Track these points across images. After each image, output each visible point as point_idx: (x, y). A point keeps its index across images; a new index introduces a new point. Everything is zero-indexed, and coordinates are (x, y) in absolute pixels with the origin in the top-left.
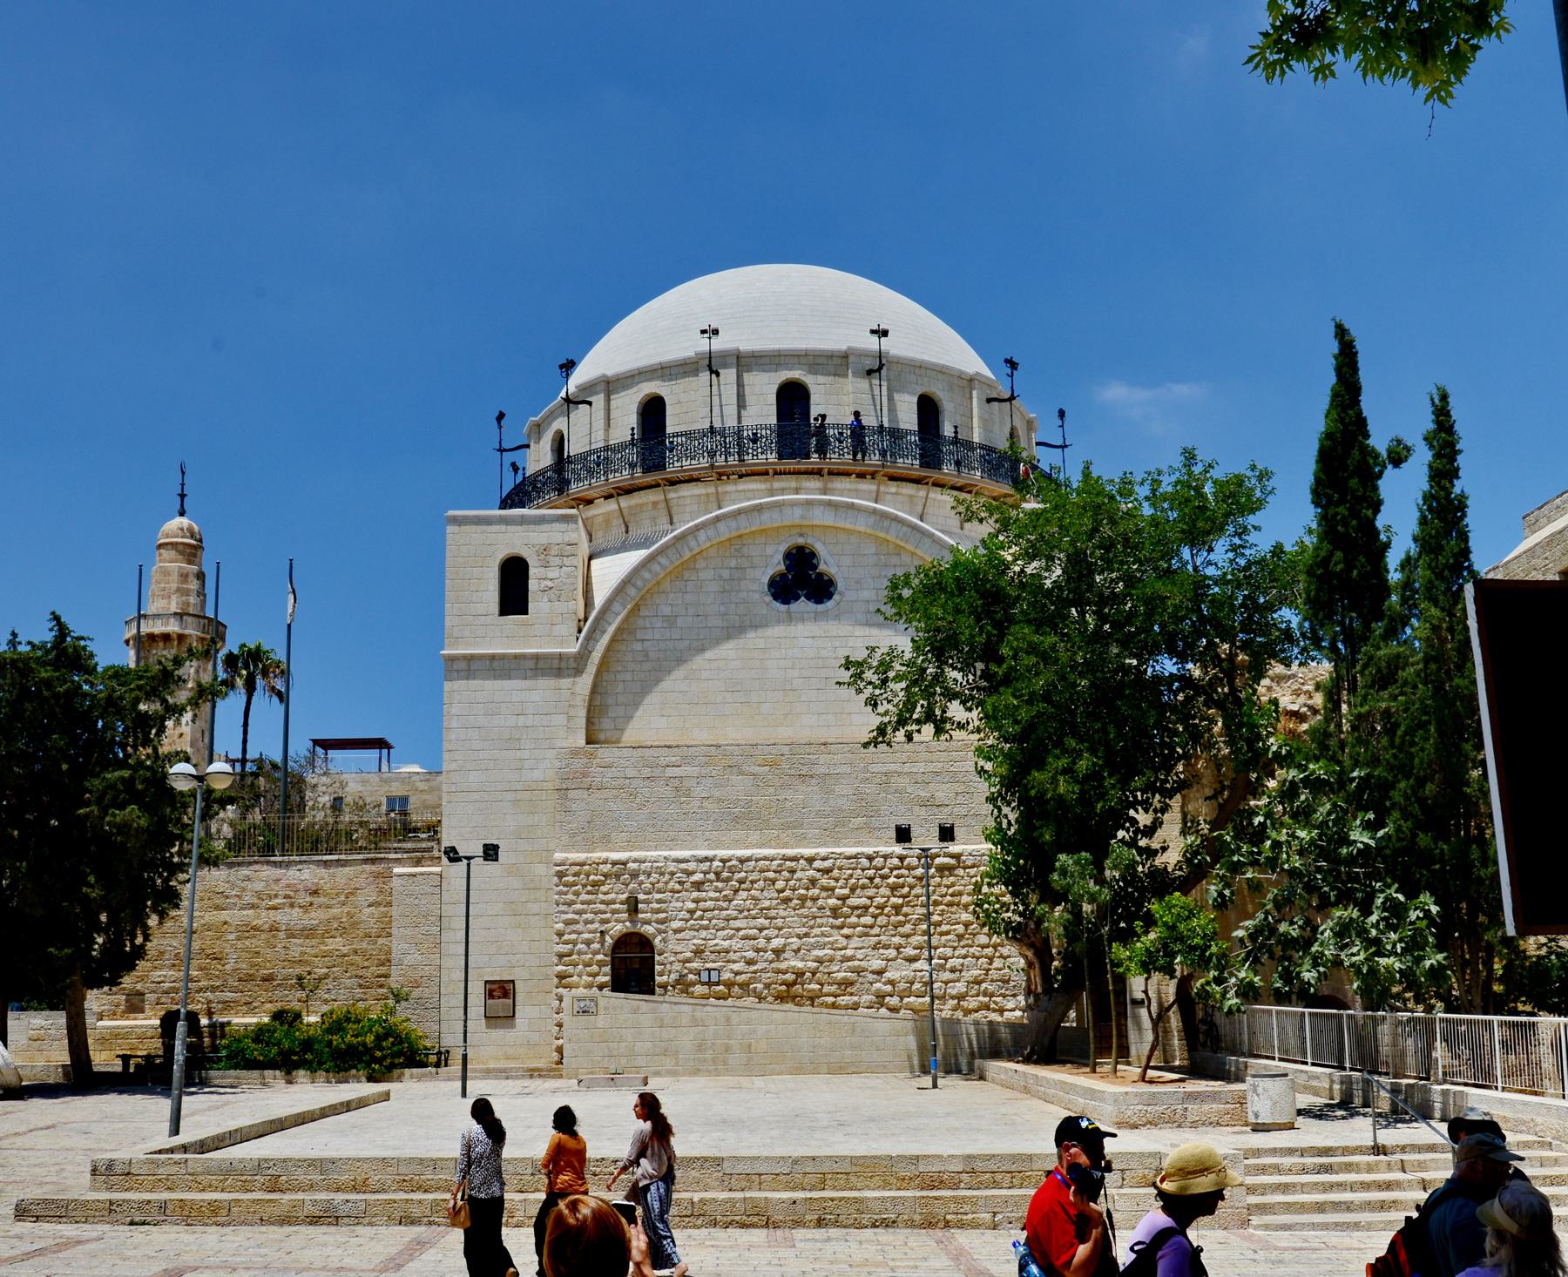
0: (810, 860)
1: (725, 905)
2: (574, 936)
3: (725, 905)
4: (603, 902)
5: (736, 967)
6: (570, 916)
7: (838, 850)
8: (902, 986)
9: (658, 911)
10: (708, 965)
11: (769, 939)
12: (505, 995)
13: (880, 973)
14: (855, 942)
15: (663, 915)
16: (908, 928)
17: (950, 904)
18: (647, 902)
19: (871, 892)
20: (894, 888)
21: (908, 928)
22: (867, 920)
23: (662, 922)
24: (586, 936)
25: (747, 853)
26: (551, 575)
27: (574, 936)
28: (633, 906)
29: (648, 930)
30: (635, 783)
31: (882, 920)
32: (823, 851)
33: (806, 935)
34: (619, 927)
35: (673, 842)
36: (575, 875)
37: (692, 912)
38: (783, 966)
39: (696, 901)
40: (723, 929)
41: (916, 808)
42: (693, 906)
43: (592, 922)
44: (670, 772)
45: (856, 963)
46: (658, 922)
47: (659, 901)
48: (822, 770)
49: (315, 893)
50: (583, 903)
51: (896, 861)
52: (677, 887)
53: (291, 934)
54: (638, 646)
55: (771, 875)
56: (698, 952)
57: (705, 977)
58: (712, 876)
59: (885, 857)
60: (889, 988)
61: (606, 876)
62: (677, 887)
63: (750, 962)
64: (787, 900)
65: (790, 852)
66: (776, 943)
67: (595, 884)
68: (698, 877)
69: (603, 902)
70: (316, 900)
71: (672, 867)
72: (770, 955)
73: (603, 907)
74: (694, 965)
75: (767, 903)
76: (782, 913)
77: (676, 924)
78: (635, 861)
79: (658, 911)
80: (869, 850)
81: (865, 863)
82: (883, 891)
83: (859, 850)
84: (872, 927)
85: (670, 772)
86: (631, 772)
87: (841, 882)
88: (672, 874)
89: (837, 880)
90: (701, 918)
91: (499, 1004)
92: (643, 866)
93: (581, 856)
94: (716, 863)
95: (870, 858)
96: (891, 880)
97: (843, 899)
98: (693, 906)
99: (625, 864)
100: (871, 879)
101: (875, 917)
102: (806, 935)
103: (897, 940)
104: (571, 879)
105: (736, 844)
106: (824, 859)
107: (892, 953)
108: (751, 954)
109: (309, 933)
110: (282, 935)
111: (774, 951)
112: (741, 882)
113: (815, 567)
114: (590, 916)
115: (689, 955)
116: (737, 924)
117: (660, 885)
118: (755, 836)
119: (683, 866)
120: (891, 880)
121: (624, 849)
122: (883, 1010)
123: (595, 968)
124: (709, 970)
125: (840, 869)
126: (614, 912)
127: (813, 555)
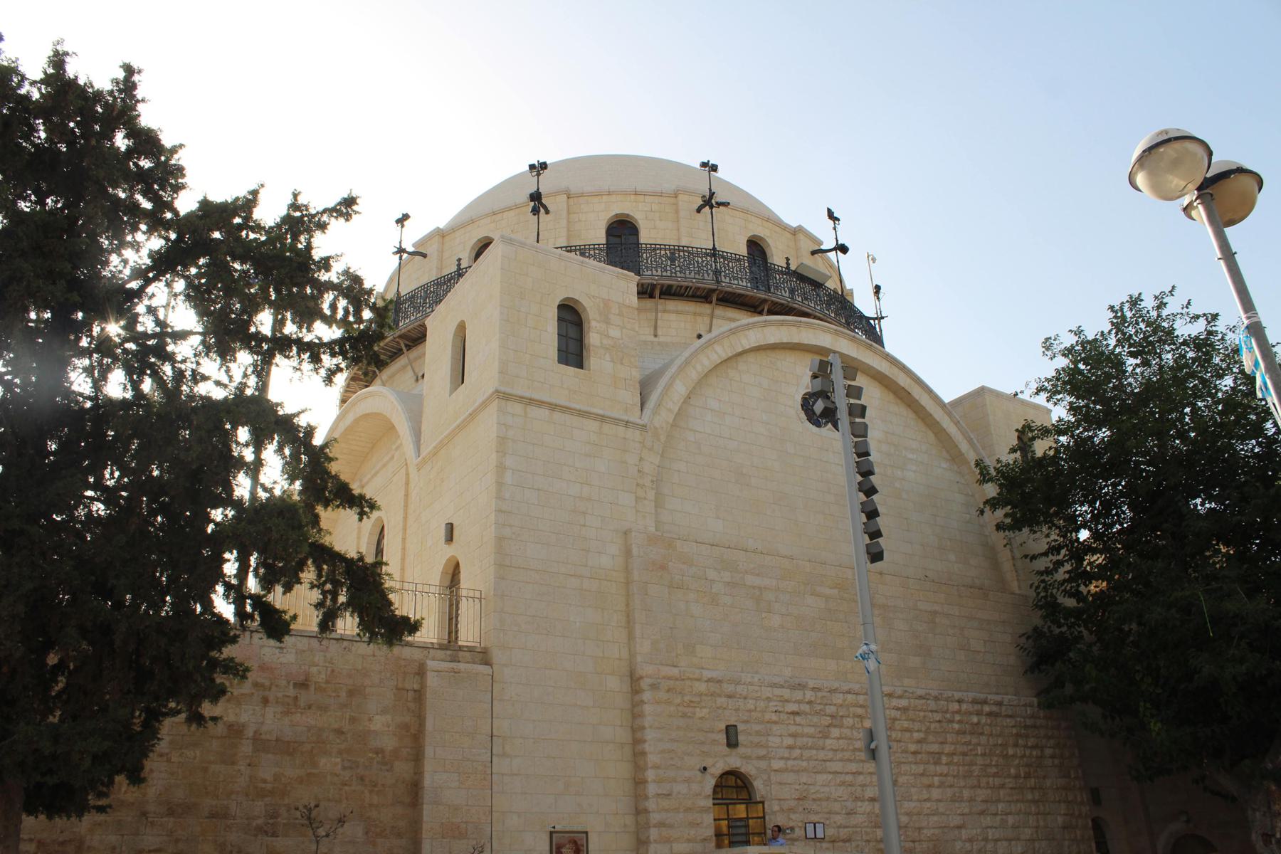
1: (821, 742)
5: (839, 819)
9: (758, 745)
13: (959, 827)
14: (936, 793)
15: (762, 752)
20: (959, 732)
22: (944, 769)
24: (687, 774)
25: (836, 685)
29: (747, 769)
32: (899, 691)
37: (790, 748)
39: (794, 736)
44: (751, 580)
46: (759, 758)
47: (758, 733)
49: (303, 685)
51: (956, 706)
52: (774, 717)
53: (260, 744)
55: (860, 711)
61: (701, 695)
63: (850, 813)
68: (794, 707)
69: (700, 730)
70: (304, 698)
71: (767, 692)
77: (777, 764)
86: (712, 574)
90: (801, 758)
98: (790, 741)
106: (900, 697)
108: (850, 805)
109: (285, 748)
110: (246, 748)
112: (832, 716)
115: (793, 803)
116: (837, 766)
119: (778, 692)
120: (956, 726)
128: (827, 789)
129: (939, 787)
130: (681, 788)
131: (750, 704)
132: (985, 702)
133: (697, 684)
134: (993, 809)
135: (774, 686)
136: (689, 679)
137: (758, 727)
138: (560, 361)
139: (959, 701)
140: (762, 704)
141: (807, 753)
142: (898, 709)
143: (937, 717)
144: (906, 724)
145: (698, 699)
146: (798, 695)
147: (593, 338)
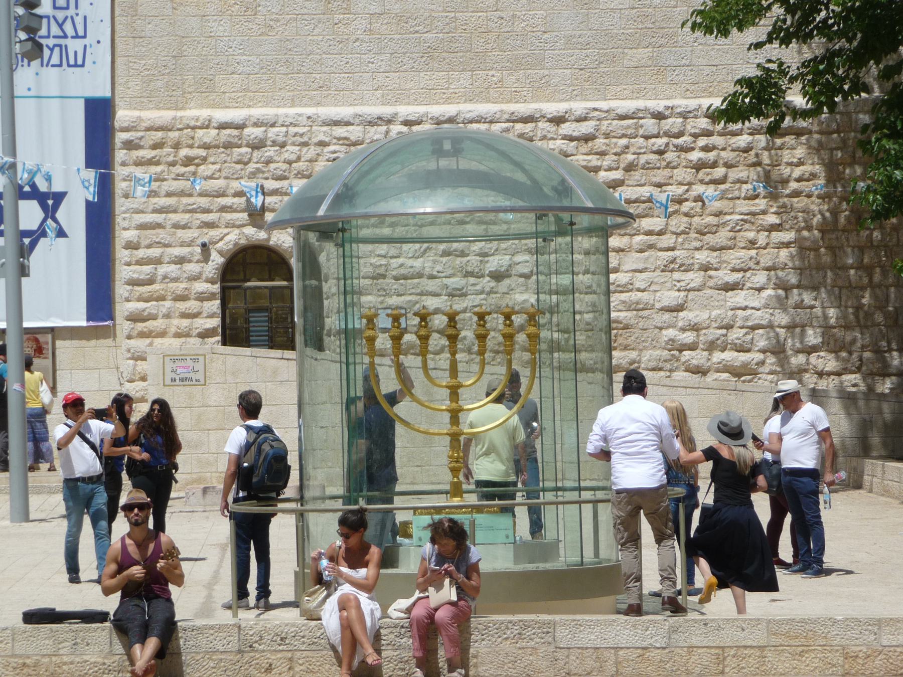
0: (558, 120)
2: (155, 252)
7: (604, 105)
8: (714, 333)
16: (722, 237)
19: (660, 176)
20: (699, 166)
21: (722, 237)
24: (177, 251)
25: (450, 110)
31: (678, 223)
32: (579, 107)
36: (155, 147)
45: (635, 296)
50: (169, 195)
59: (685, 115)
60: (688, 337)
61: (206, 146)
65: (523, 109)
67: (189, 161)
72: (487, 283)
73: (204, 202)
80: (658, 105)
81: (650, 124)
82: (681, 174)
83: (640, 104)
84: (661, 233)
87: (607, 161)
88: (322, 144)
92: (272, 133)
93: (165, 116)
95: (659, 116)
99: (241, 127)
103: (702, 257)
104: (147, 154)
105: (429, 95)
106: (580, 120)
107: (694, 278)
108: (456, 282)
114: (183, 218)
117: (301, 165)
118: (463, 81)
119: (340, 131)
120: (695, 156)
121: (238, 104)
122: (680, 376)
123: (192, 305)
125: (607, 136)
126: (224, 209)
129: (641, 251)
130: (172, 270)
131: (291, 151)
133: (200, 133)
135: (337, 123)
140: (311, 152)
142: (571, 139)
143: (661, 142)
144: (580, 159)
145: (202, 153)
146: (376, 133)
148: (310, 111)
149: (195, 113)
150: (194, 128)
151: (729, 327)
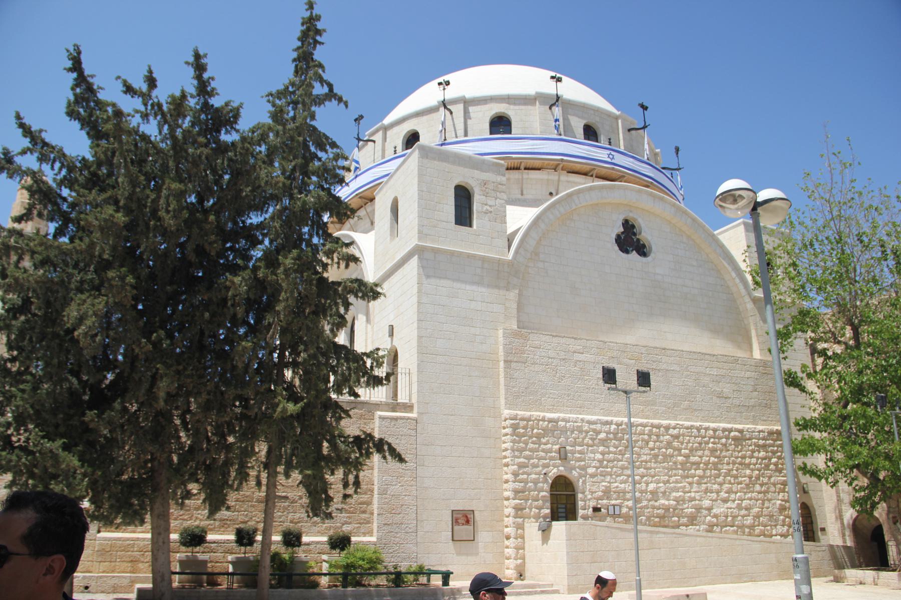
3: (620, 457)
4: (543, 451)
6: (522, 460)
9: (580, 460)
10: (613, 502)
11: (647, 484)
12: (468, 522)
13: (709, 509)
17: (741, 464)
18: (573, 452)
21: (721, 479)
23: (584, 468)
24: (533, 476)
26: (490, 203)
27: (525, 476)
28: (563, 455)
30: (555, 362)
31: (708, 473)
32: (673, 423)
33: (668, 482)
34: (555, 470)
35: (581, 409)
38: (657, 504)
39: (603, 454)
40: (620, 475)
41: (714, 398)
42: (600, 457)
43: (537, 466)
47: (580, 452)
48: (664, 366)
51: (711, 432)
54: (541, 265)
56: (607, 493)
57: (611, 512)
58: (611, 436)
62: (590, 442)
64: (656, 456)
65: (656, 422)
66: (652, 486)
67: (539, 436)
69: (543, 451)
72: (649, 496)
73: (543, 454)
74: (605, 501)
75: (644, 458)
76: (653, 465)
77: (591, 470)
78: (564, 420)
79: (580, 460)
85: (577, 357)
86: (552, 354)
88: (587, 432)
89: (682, 443)
91: (463, 530)
94: (613, 427)
96: (711, 445)
97: (687, 456)
98: (600, 457)
100: (700, 444)
101: (704, 470)
102: (668, 482)
103: (716, 487)
106: (674, 428)
107: (714, 496)
111: (652, 492)
113: (635, 234)
115: (600, 494)
124: (614, 506)
126: (552, 458)
127: (633, 226)
128: (623, 486)
132: (730, 430)
134: (733, 496)
136: (536, 419)
137: (578, 448)
138: (456, 223)
139: (715, 430)
141: (610, 464)
146: (606, 428)
147: (476, 207)
148: (581, 416)
149: (536, 414)
150: (539, 420)
151: (727, 517)
